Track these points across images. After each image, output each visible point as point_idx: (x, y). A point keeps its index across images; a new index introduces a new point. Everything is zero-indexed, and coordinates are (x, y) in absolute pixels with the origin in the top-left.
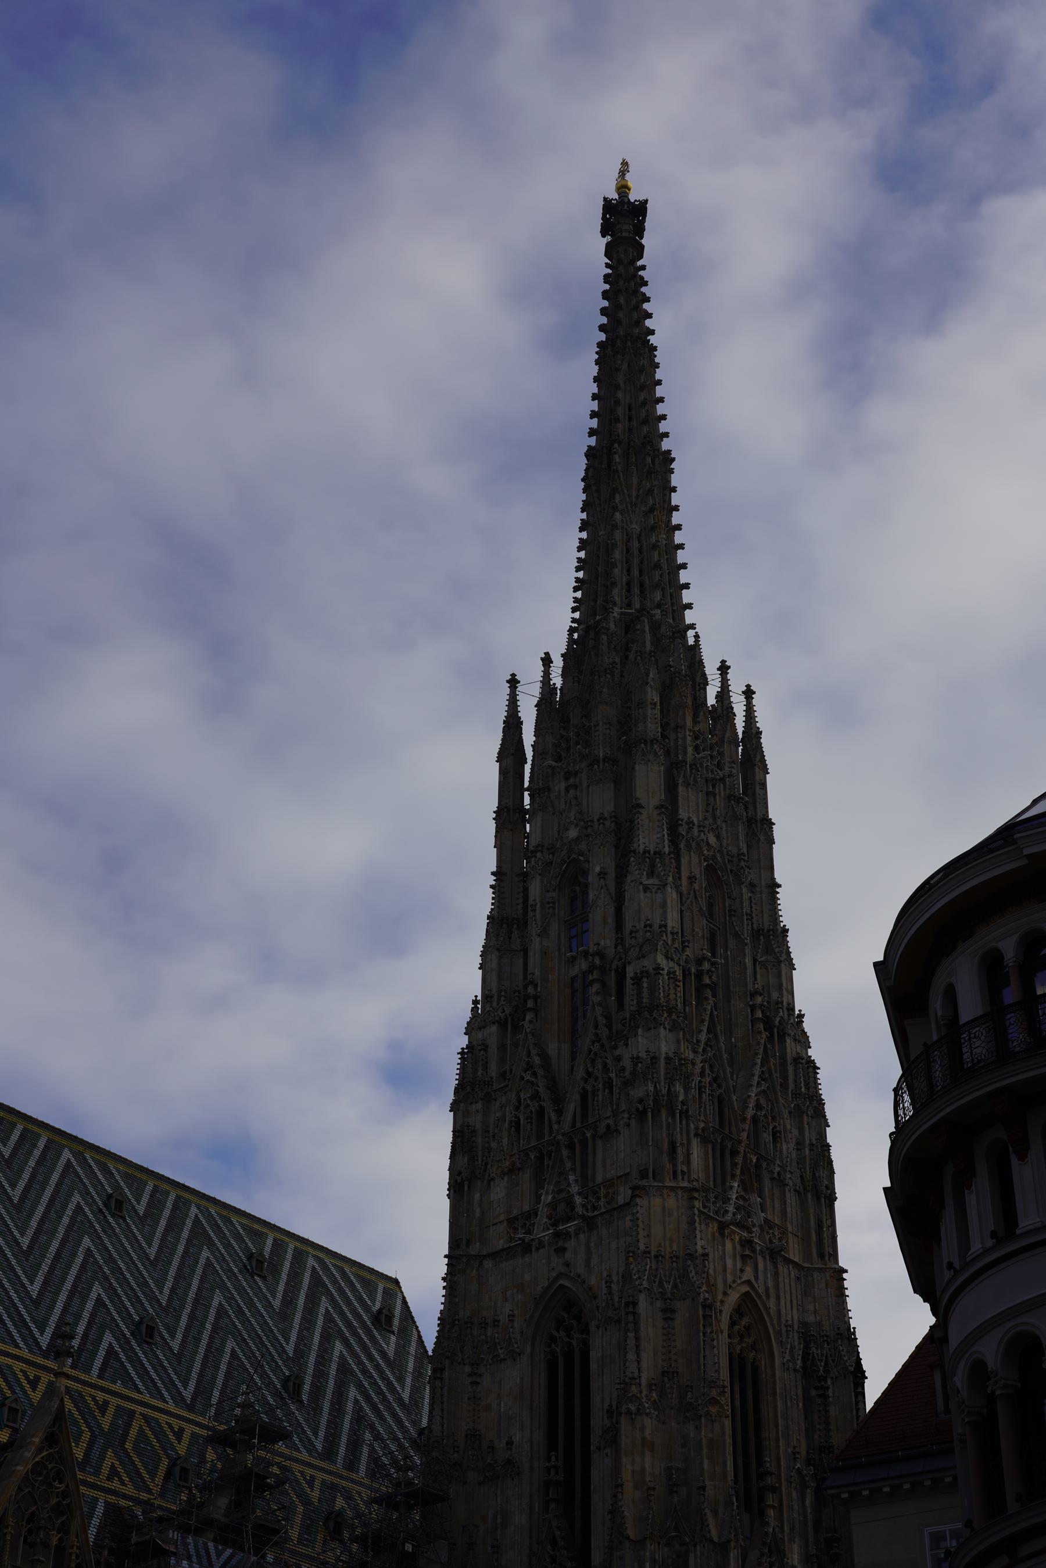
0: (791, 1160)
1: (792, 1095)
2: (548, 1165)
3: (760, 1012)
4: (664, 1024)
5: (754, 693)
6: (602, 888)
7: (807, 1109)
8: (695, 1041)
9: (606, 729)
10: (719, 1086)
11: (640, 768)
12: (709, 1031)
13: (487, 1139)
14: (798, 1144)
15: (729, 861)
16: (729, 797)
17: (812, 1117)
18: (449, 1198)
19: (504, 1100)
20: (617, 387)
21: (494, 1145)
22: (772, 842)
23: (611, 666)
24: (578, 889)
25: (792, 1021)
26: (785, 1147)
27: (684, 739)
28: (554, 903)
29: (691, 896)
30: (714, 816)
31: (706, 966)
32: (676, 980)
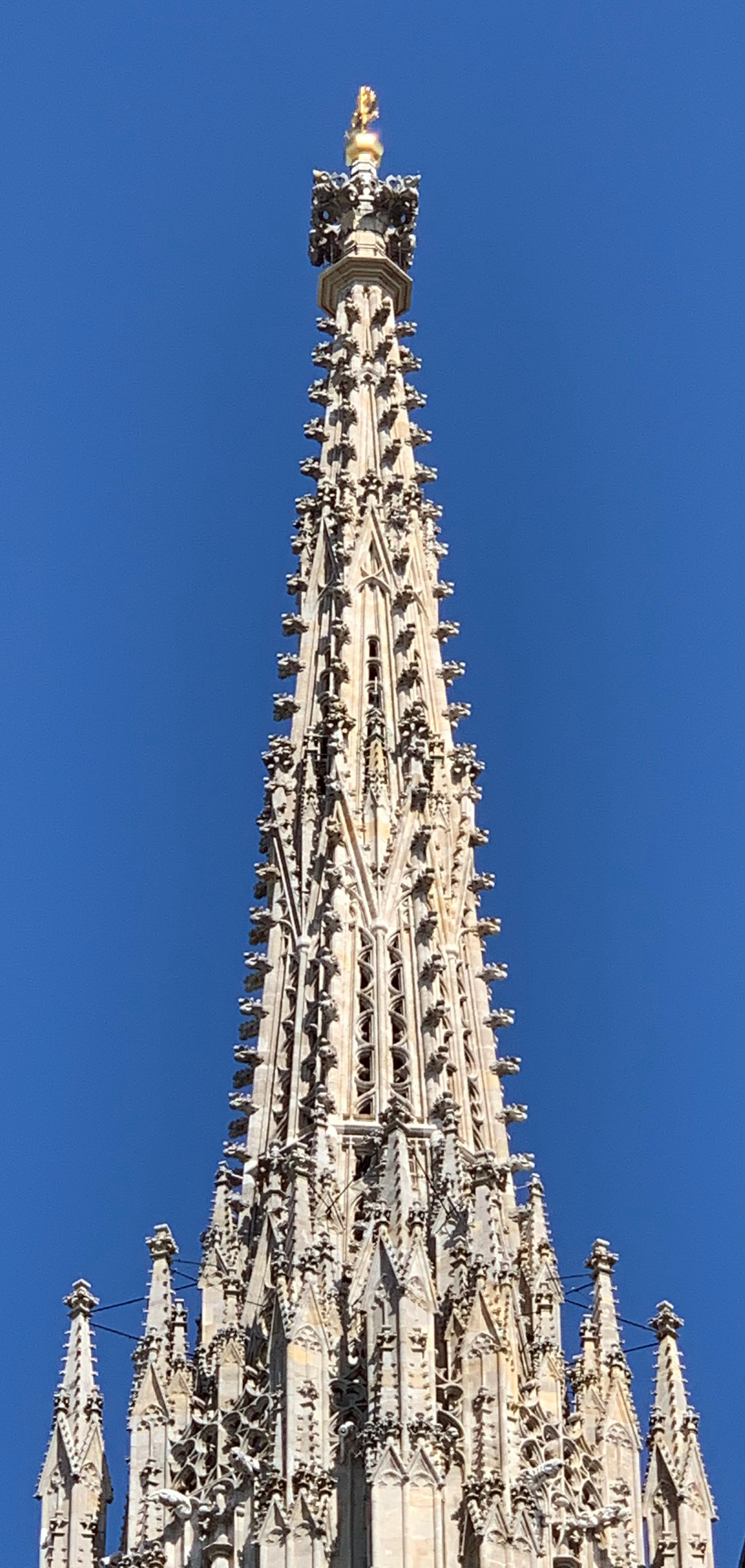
23: (317, 1253)
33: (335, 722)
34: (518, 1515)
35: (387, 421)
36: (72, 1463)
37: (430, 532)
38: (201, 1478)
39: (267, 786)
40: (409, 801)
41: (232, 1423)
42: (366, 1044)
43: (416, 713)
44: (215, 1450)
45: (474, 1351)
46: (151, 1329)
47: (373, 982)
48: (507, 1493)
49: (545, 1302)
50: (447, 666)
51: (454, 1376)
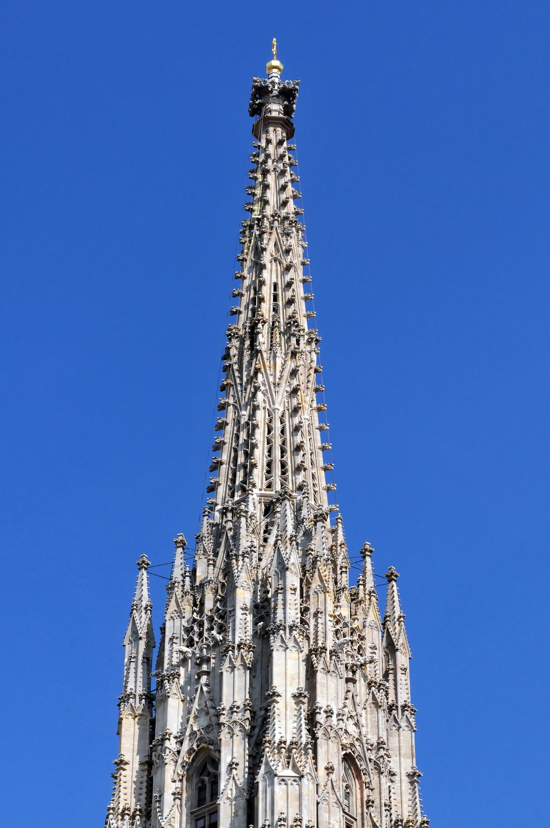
11: (278, 656)
16: (369, 685)
20: (263, 267)
23: (249, 549)
33: (259, 320)
34: (333, 662)
35: (283, 188)
36: (139, 632)
37: (300, 237)
38: (196, 642)
39: (228, 346)
40: (290, 355)
41: (211, 619)
42: (270, 459)
43: (294, 317)
44: (203, 630)
45: (315, 592)
46: (176, 578)
47: (273, 432)
48: (328, 652)
49: (344, 570)
50: (306, 295)
51: (306, 602)
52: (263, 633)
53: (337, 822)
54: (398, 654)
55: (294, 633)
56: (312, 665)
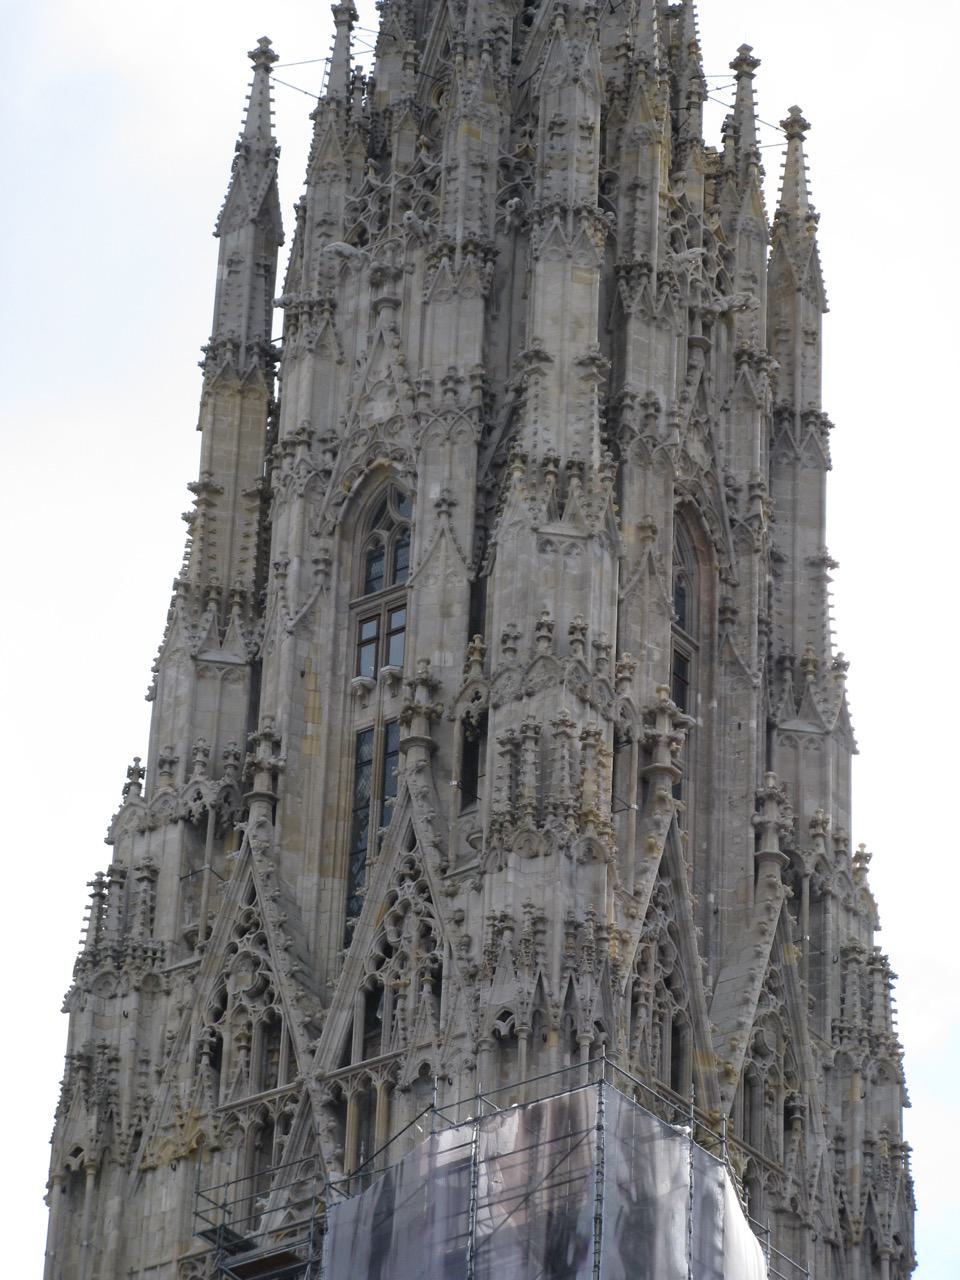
0: (822, 1173)
1: (833, 1028)
2: (281, 1146)
3: (776, 841)
4: (568, 847)
5: (806, 127)
6: (442, 534)
7: (865, 1064)
8: (632, 894)
9: (475, 177)
10: (677, 997)
12: (663, 872)
13: (143, 1078)
14: (839, 1139)
15: (729, 499)
17: (874, 1082)
18: (47, 1204)
19: (188, 995)
21: (158, 1093)
22: (824, 465)
24: (384, 535)
25: (842, 867)
26: (810, 1142)
27: (650, 214)
28: (328, 563)
29: (641, 568)
30: (702, 395)
31: (664, 729)
32: (600, 752)
45: (632, 141)
48: (654, 276)
51: (613, 160)
52: (517, 223)
53: (658, 645)
54: (801, 298)
55: (585, 224)
56: (620, 305)
